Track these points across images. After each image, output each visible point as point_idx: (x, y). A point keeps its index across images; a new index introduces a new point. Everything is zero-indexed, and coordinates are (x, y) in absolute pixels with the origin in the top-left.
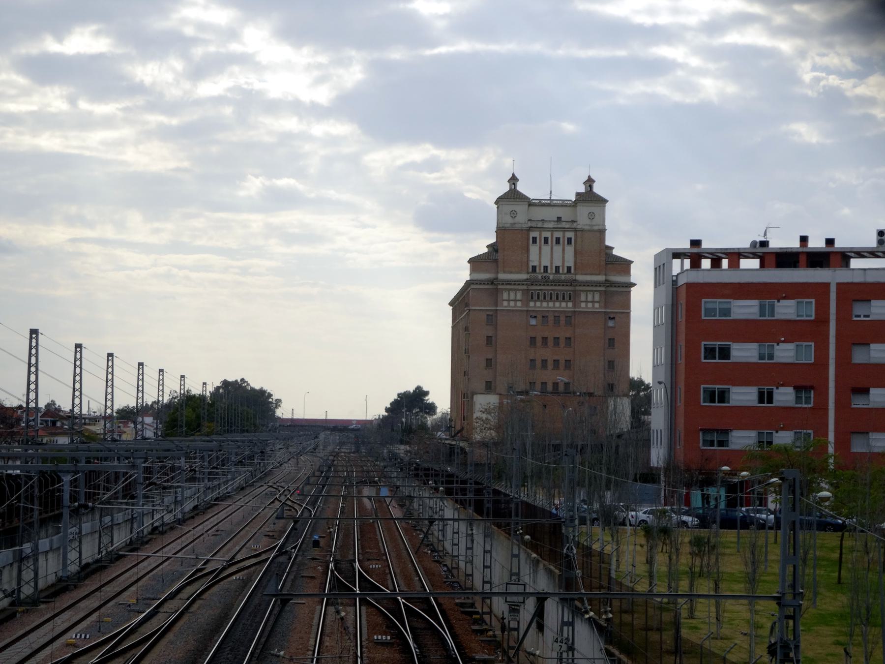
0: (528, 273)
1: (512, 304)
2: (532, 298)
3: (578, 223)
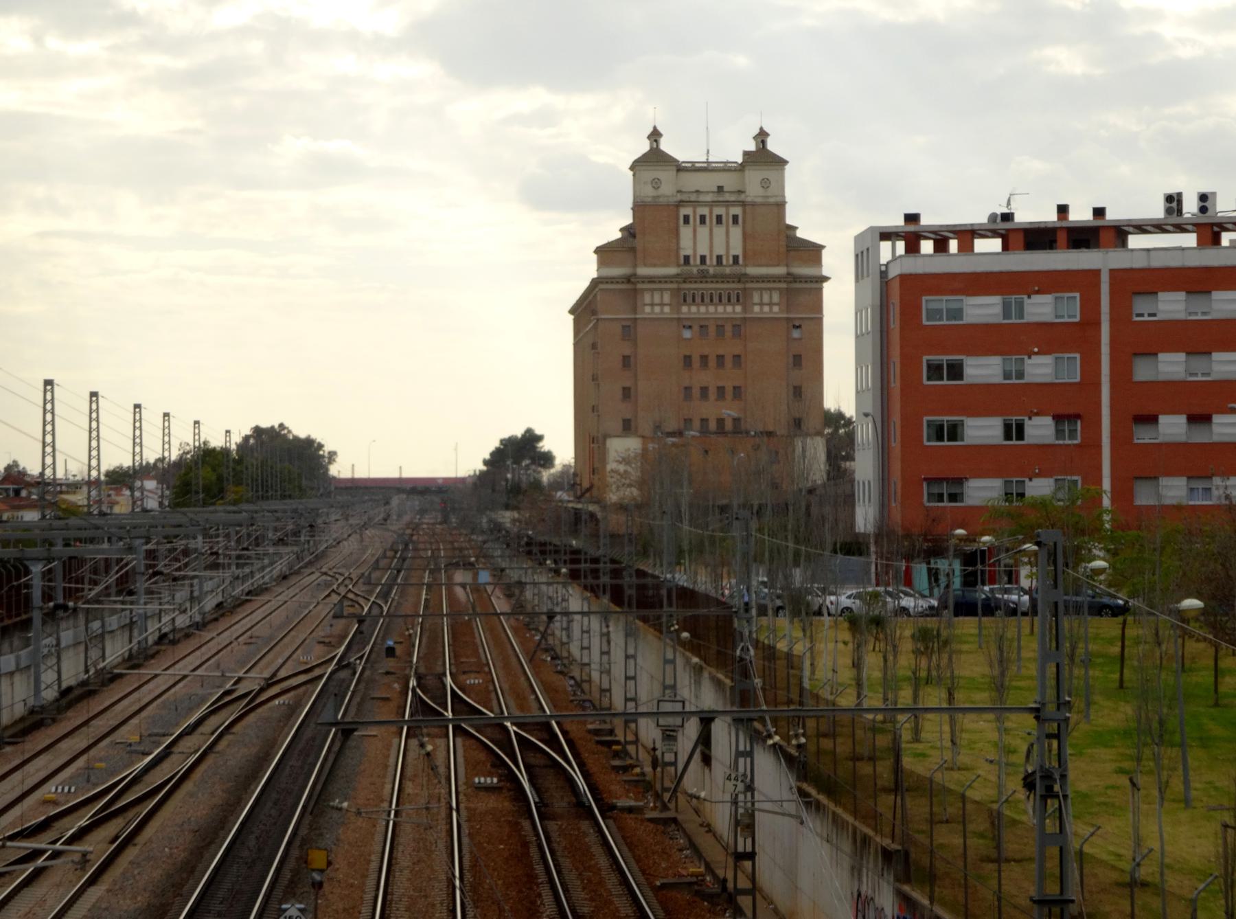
0: (679, 265)
1: (657, 309)
2: (685, 300)
3: (747, 193)
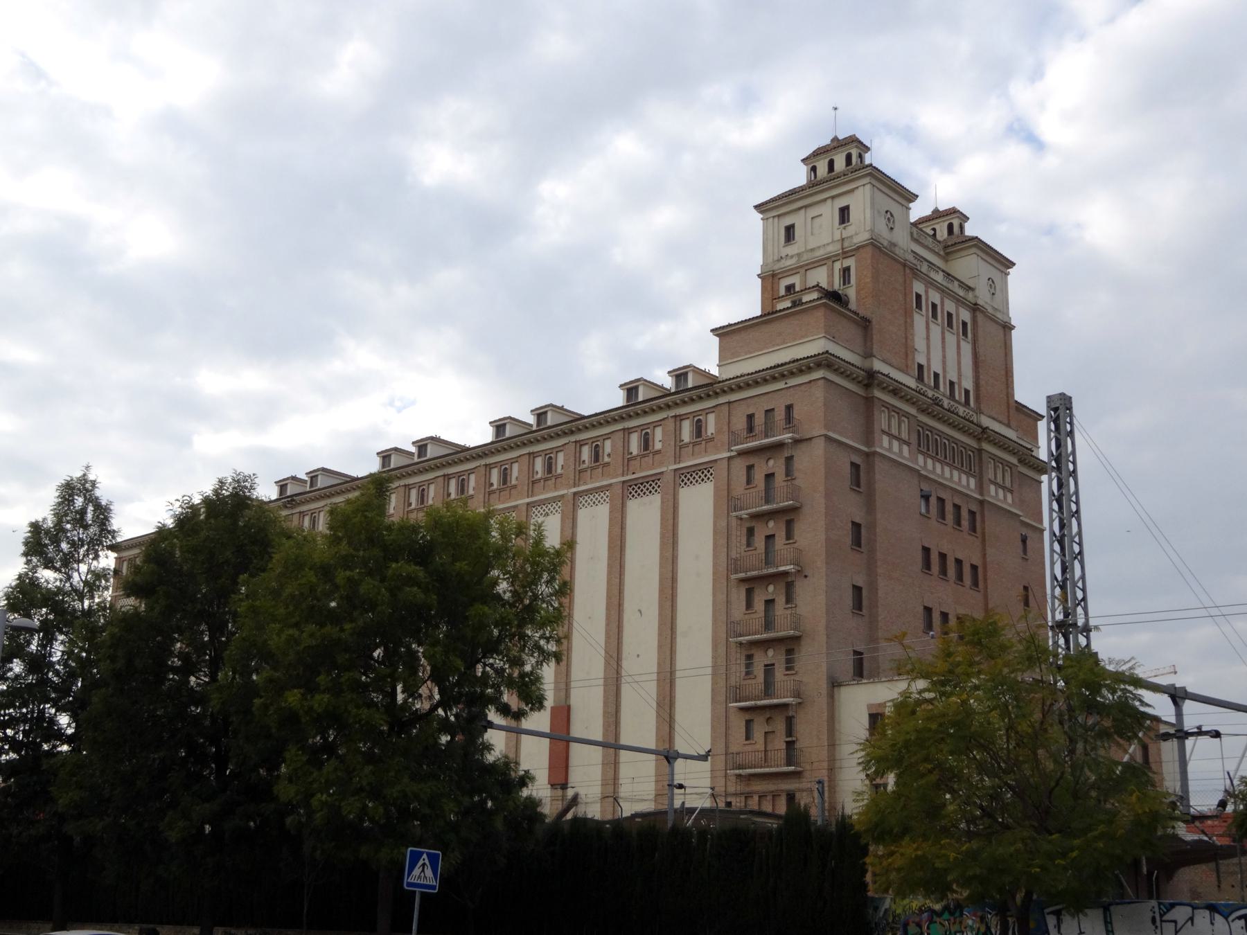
3: (977, 291)
